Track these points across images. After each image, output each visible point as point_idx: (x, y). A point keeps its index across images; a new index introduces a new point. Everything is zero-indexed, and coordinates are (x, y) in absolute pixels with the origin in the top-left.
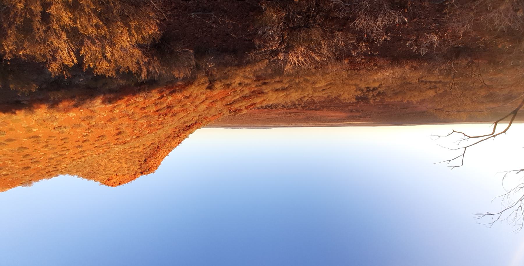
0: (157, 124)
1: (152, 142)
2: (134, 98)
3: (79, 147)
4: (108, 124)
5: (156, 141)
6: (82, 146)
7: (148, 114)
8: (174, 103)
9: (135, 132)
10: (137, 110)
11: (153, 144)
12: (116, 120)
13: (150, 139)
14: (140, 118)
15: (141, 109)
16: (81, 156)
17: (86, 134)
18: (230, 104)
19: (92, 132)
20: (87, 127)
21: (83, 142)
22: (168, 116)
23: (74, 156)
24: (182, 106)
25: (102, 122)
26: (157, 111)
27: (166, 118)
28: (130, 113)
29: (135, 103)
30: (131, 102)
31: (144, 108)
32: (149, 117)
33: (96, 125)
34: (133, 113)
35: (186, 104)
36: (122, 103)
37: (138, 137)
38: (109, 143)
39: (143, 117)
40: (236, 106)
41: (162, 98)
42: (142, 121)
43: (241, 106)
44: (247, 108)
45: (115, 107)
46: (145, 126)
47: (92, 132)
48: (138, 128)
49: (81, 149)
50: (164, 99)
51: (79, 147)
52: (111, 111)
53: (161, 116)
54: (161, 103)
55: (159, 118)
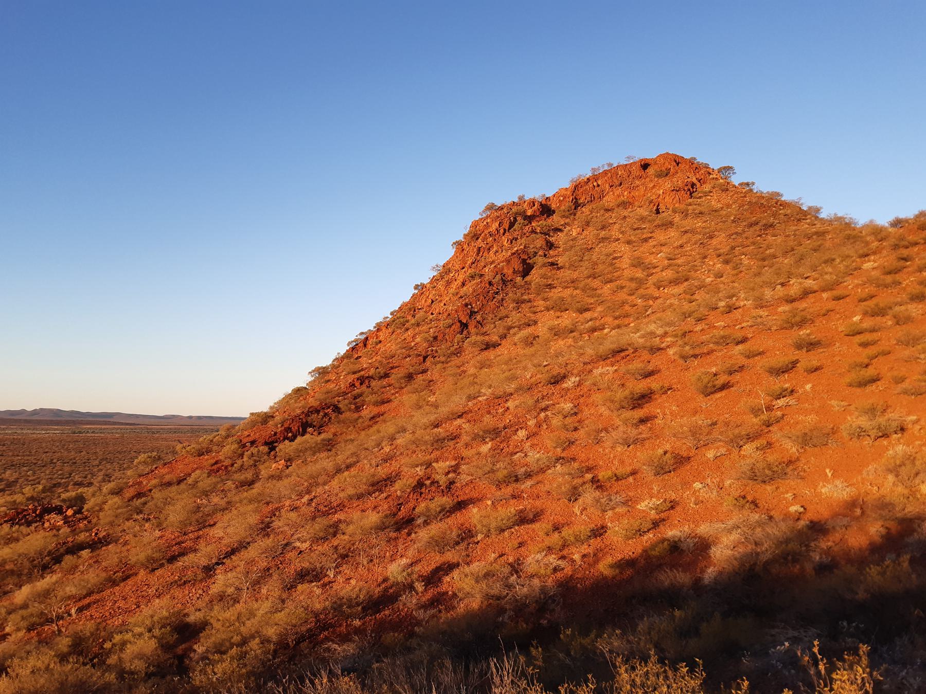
0: (465, 438)
1: (491, 354)
2: (568, 571)
3: (811, 345)
4: (685, 446)
5: (471, 358)
6: (799, 347)
7: (508, 490)
8: (379, 544)
9: (568, 406)
10: (554, 510)
11: (488, 346)
12: (650, 463)
13: (500, 371)
14: (542, 471)
15: (537, 516)
16: (803, 305)
17: (781, 402)
18: (75, 549)
19: (756, 411)
20: (776, 434)
21: (794, 364)
22: (413, 482)
23: (832, 305)
24: (335, 530)
25: (710, 454)
26: (461, 506)
27: (420, 471)
28: (589, 496)
29: (564, 546)
30: (584, 549)
31: (523, 519)
32: (500, 475)
33: (736, 443)
34: (574, 495)
35: (317, 540)
36: (623, 542)
37: (556, 380)
39: (529, 475)
40: (35, 540)
41: (438, 570)
42: (534, 456)
45: (656, 524)
46: (522, 434)
47: (756, 411)
48: (556, 422)
49: (803, 332)
50: (425, 568)
51: (811, 345)
52: (673, 505)
53: (443, 480)
54: (439, 544)
55: (455, 469)
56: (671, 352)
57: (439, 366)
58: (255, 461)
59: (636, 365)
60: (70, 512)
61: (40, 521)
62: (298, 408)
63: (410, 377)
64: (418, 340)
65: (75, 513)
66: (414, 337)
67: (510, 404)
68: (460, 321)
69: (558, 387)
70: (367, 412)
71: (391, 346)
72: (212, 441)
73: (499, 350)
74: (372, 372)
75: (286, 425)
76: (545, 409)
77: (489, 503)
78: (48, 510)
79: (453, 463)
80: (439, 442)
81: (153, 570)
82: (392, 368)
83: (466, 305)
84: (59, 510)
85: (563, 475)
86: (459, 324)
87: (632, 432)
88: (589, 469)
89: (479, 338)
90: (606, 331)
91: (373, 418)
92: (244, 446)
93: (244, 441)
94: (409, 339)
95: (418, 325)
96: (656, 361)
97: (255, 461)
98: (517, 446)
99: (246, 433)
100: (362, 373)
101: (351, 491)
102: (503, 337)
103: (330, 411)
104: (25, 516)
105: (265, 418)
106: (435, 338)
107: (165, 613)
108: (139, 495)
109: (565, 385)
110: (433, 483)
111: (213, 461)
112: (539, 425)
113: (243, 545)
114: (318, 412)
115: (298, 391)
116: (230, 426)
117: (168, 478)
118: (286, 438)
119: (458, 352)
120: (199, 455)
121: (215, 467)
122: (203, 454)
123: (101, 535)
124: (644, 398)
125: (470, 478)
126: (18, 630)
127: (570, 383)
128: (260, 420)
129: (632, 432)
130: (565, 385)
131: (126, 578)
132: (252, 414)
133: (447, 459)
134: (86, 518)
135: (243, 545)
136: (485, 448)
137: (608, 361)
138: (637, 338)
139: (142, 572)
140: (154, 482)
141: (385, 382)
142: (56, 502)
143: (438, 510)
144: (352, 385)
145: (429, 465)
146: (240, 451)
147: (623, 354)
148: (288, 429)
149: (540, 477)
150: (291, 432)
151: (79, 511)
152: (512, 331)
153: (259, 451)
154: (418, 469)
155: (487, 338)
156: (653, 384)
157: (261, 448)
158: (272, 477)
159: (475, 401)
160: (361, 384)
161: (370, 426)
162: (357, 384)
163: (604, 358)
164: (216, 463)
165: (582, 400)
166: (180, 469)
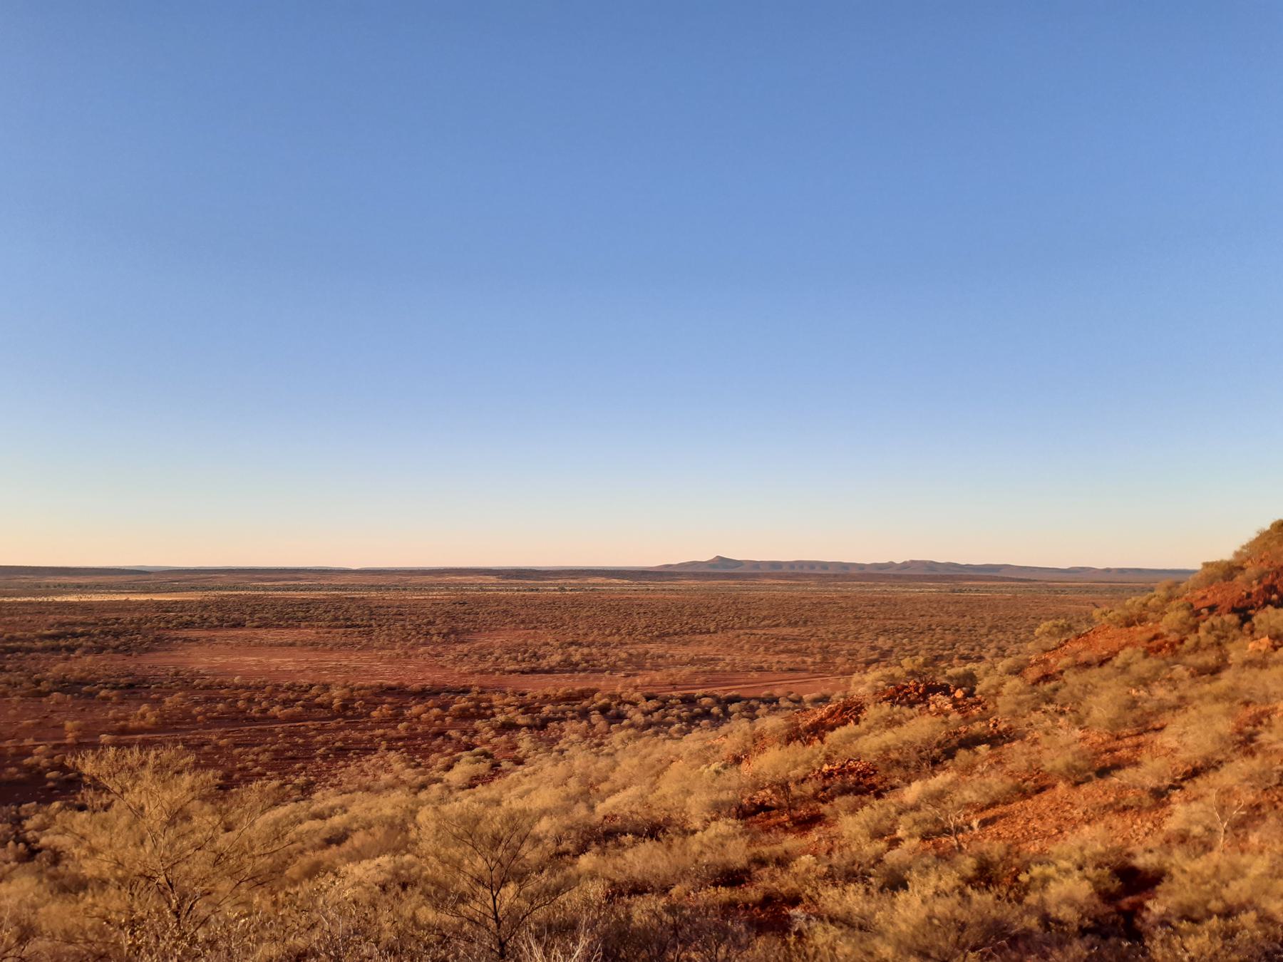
18: (971, 742)
40: (921, 727)
43: (891, 723)
44: (851, 710)
58: (1219, 637)
60: (959, 694)
61: (923, 702)
65: (966, 695)
75: (1267, 582)
78: (932, 689)
81: (1077, 784)
84: (946, 690)
92: (1197, 613)
93: (1198, 605)
97: (1219, 637)
99: (1200, 594)
104: (906, 694)
105: (1229, 571)
107: (1100, 848)
108: (1046, 678)
111: (1151, 635)
116: (1174, 581)
117: (1084, 657)
118: (1268, 602)
121: (1155, 644)
122: (1133, 624)
123: (1002, 727)
126: (911, 836)
128: (1221, 573)
131: (1040, 790)
132: (1206, 565)
134: (979, 703)
139: (1061, 786)
140: (1066, 661)
142: (941, 680)
146: (1191, 621)
150: (1276, 592)
151: (970, 693)
153: (1223, 622)
157: (1227, 617)
158: (1249, 663)
164: (1156, 637)
166: (1101, 646)
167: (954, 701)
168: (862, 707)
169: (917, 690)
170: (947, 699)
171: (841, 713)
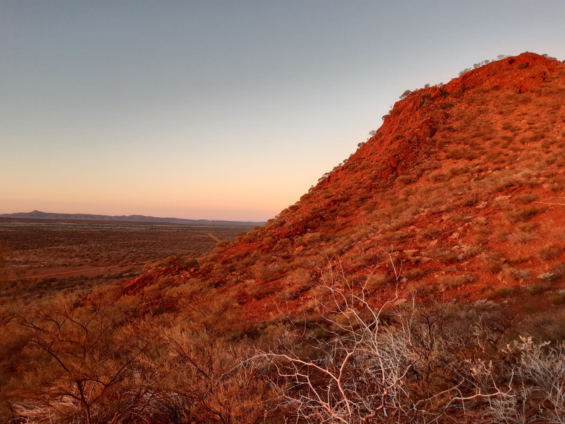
0: (418, 237)
1: (413, 187)
11: (409, 182)
13: (422, 196)
27: (396, 254)
28: (507, 270)
38: (554, 190)
39: (465, 259)
46: (455, 235)
56: (545, 186)
57: (380, 194)
59: (523, 195)
60: (192, 270)
61: (178, 274)
62: (299, 217)
63: (363, 200)
64: (365, 178)
65: (195, 270)
66: (362, 176)
67: (444, 218)
68: (391, 166)
69: (473, 208)
70: (339, 221)
71: (348, 181)
72: (256, 235)
73: (418, 185)
74: (339, 197)
76: (467, 221)
77: (443, 272)
78: (181, 269)
79: (414, 251)
80: (403, 240)
82: (351, 195)
83: (395, 156)
85: (487, 259)
86: (390, 168)
87: (527, 235)
88: (503, 255)
89: (405, 177)
90: (490, 171)
91: (343, 224)
93: (274, 235)
94: (359, 177)
95: (363, 169)
96: (535, 193)
98: (453, 242)
99: (273, 231)
100: (333, 198)
101: (359, 263)
102: (420, 176)
103: (318, 219)
106: (376, 177)
108: (225, 262)
109: (478, 207)
110: (406, 262)
111: (259, 245)
112: (465, 231)
113: (304, 290)
114: (312, 220)
115: (294, 208)
117: (237, 254)
118: (296, 234)
119: (392, 185)
120: (250, 242)
124: (530, 215)
125: (430, 259)
127: (481, 205)
129: (527, 235)
130: (478, 207)
133: (410, 249)
134: (200, 273)
135: (304, 290)
136: (434, 243)
137: (504, 192)
138: (518, 176)
141: (347, 204)
143: (416, 275)
144: (329, 205)
145: (401, 251)
147: (512, 188)
148: (297, 230)
149: (472, 259)
152: (426, 172)
154: (395, 253)
155: (409, 176)
156: (537, 205)
157: (286, 239)
159: (418, 216)
160: (334, 204)
161: (342, 229)
162: (332, 204)
163: (500, 190)
164: (261, 246)
165: (490, 216)
167: (190, 273)
168: (152, 278)
169: (175, 269)
170: (187, 273)
171: (143, 281)
